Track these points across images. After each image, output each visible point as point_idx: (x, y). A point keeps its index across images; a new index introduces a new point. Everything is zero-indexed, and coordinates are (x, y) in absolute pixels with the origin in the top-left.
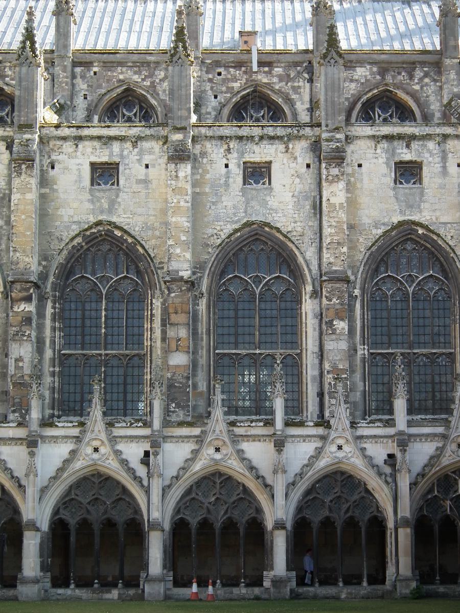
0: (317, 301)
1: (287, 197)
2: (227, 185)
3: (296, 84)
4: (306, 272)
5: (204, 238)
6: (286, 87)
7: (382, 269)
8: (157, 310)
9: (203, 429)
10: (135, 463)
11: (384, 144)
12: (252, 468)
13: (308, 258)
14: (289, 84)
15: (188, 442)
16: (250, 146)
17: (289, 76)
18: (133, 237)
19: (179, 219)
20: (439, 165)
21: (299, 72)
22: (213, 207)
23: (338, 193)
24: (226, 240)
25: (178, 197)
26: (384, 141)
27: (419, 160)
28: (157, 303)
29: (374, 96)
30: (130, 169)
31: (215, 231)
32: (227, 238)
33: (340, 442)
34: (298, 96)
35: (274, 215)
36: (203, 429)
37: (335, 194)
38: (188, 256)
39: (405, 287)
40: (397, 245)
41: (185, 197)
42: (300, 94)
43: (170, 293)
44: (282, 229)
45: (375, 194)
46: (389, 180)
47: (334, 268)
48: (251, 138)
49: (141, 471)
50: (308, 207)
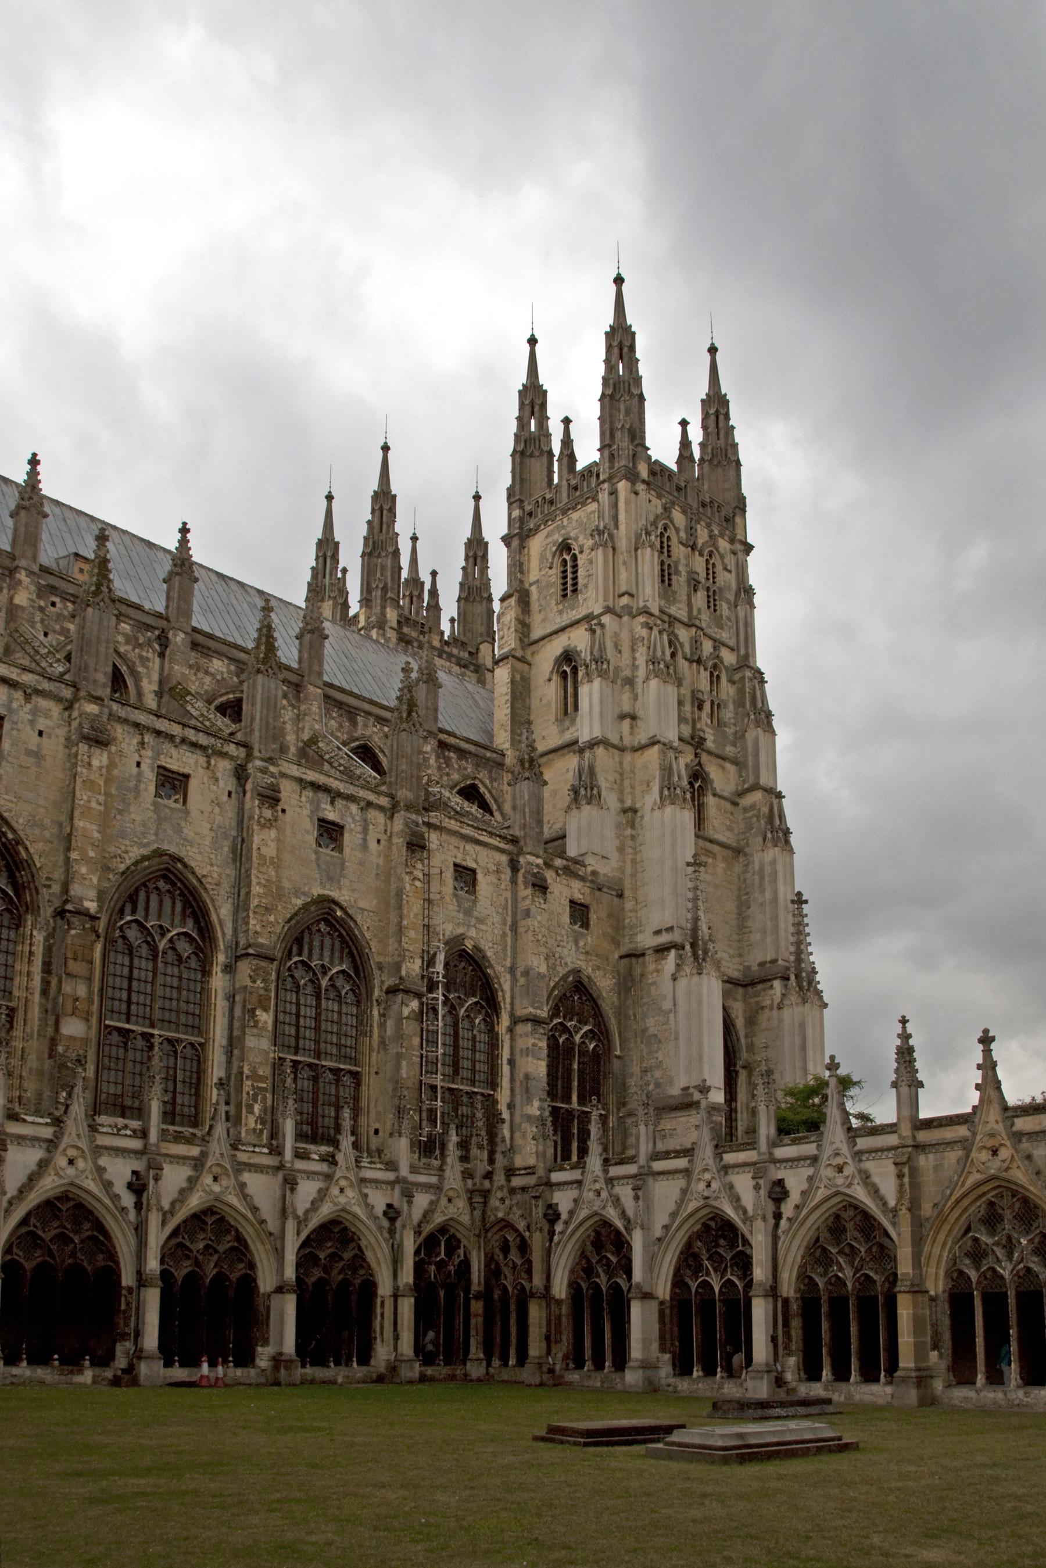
0: (228, 977)
1: (205, 828)
2: (137, 792)
3: (144, 654)
4: (219, 935)
5: (105, 857)
6: (134, 655)
7: (295, 949)
8: (38, 946)
9: (204, 1149)
10: (120, 1188)
11: (309, 793)
12: (255, 1210)
13: (222, 917)
14: (137, 651)
15: (184, 1164)
16: (167, 746)
17: (137, 639)
18: (14, 831)
19: (88, 825)
20: (359, 836)
21: (149, 640)
22: (118, 817)
23: (269, 842)
24: (133, 868)
25: (89, 794)
26: (309, 789)
27: (341, 822)
28: (39, 937)
29: (228, 702)
30: (19, 730)
31: (119, 852)
32: (133, 864)
33: (343, 1183)
34: (145, 671)
35: (189, 848)
36: (204, 1149)
37: (264, 842)
38: (95, 881)
39: (318, 979)
40: (312, 924)
41: (98, 796)
42: (147, 668)
43: (70, 928)
44: (197, 869)
45: (297, 852)
46: (311, 838)
47: (260, 940)
48: (171, 738)
49: (128, 1200)
50: (226, 849)
